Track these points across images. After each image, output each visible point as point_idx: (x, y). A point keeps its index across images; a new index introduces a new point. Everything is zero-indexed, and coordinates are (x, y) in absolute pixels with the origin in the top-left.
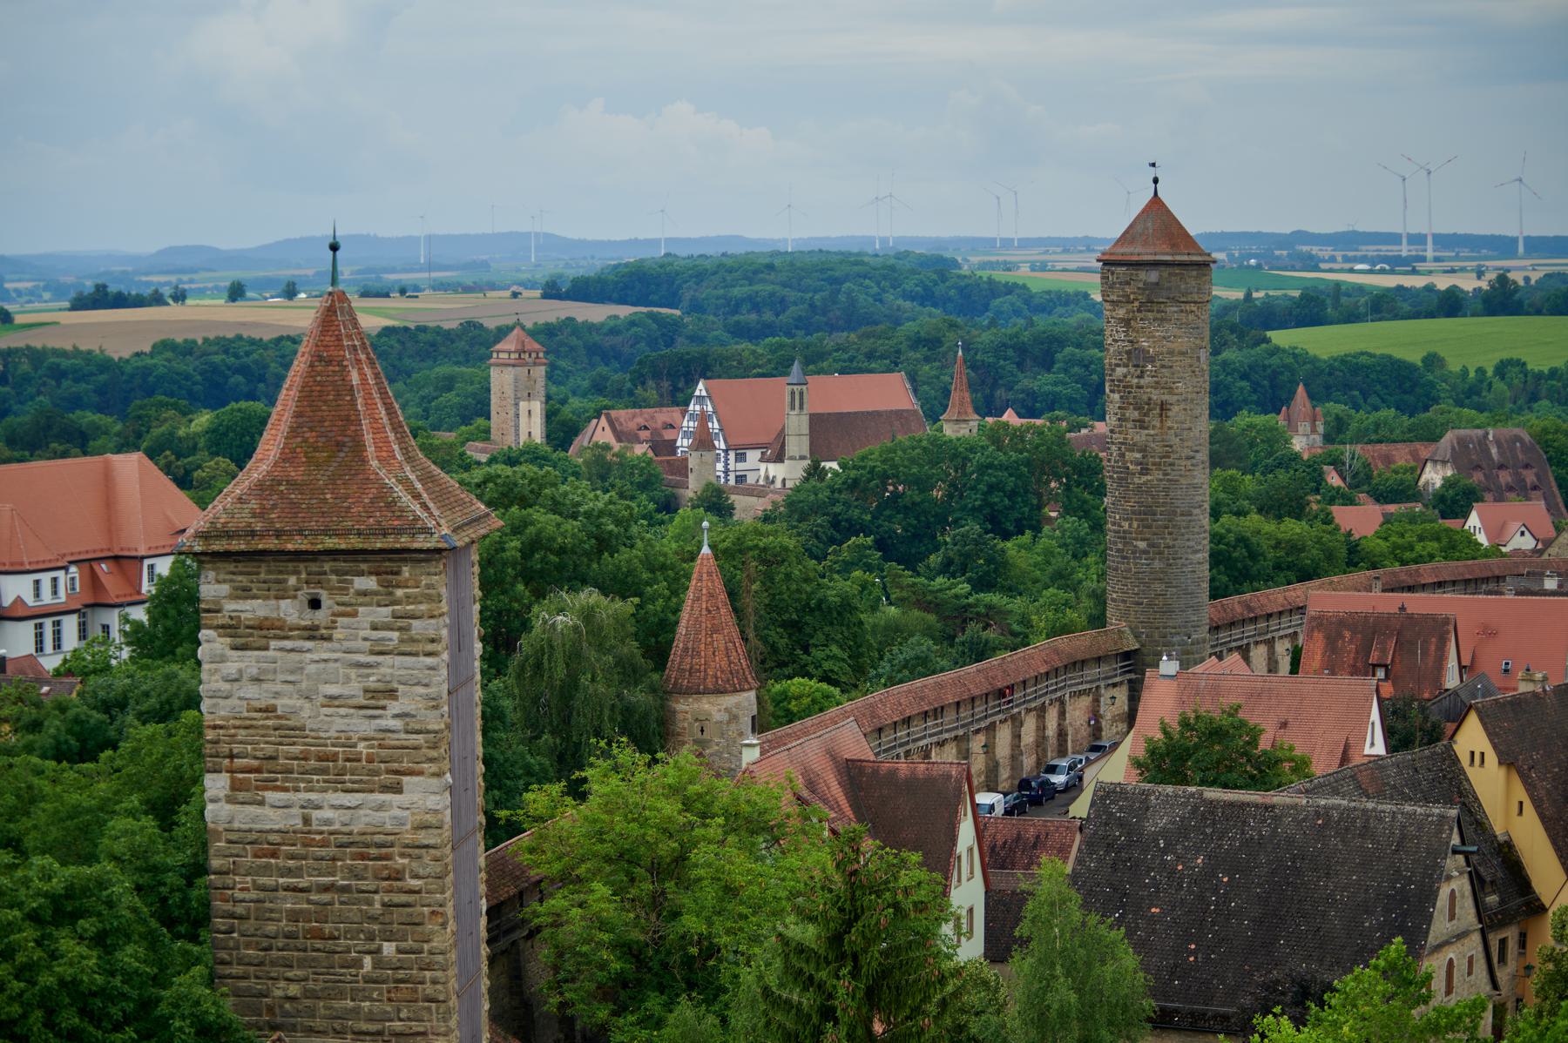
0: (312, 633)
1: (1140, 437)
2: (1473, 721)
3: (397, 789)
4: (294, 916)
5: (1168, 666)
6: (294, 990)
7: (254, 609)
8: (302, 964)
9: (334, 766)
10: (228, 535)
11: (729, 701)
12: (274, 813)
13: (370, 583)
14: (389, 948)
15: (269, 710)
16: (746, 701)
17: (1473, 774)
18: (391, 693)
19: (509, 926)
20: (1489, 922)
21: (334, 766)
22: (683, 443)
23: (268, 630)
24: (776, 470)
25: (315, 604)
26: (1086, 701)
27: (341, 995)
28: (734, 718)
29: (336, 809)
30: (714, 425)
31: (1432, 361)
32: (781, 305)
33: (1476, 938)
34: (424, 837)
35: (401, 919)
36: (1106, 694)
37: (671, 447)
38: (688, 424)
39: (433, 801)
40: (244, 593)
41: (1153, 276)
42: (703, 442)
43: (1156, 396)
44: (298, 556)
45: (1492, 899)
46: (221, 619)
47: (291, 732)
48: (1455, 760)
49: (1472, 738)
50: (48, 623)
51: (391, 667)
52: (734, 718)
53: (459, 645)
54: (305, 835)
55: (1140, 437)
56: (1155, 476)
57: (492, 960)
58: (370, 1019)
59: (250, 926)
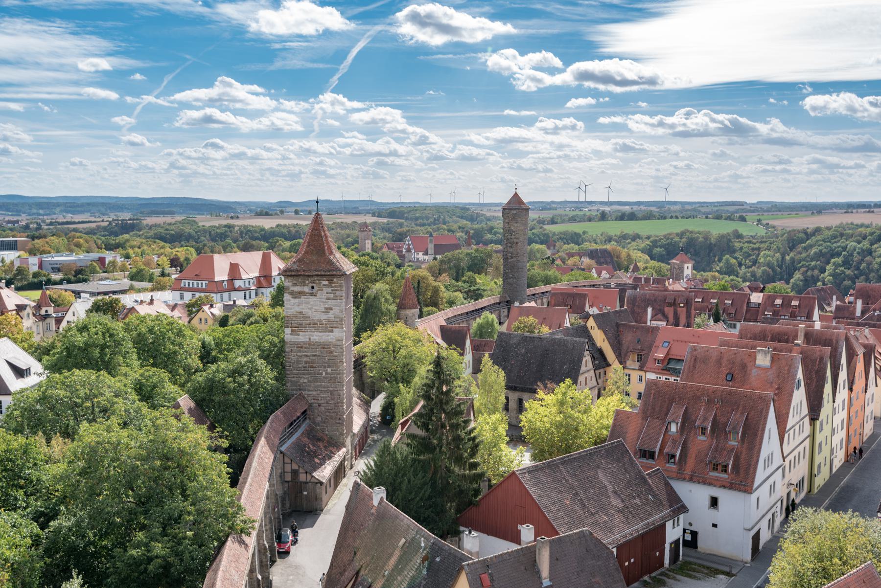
0: (312, 294)
1: (511, 250)
2: (591, 319)
3: (332, 331)
4: (306, 362)
5: (517, 304)
6: (305, 381)
7: (297, 289)
8: (308, 374)
9: (316, 326)
10: (291, 271)
11: (413, 311)
12: (302, 337)
13: (326, 283)
14: (329, 370)
15: (301, 313)
16: (417, 311)
17: (592, 331)
18: (331, 309)
19: (359, 364)
20: (596, 368)
21: (316, 326)
22: (404, 251)
23: (301, 293)
24: (426, 257)
25: (313, 288)
26: (497, 312)
27: (317, 381)
28: (414, 315)
29: (317, 337)
30: (411, 247)
31: (584, 233)
32: (427, 218)
33: (592, 372)
34: (338, 343)
35: (334, 363)
36: (502, 311)
37: (402, 252)
38: (406, 246)
39: (341, 334)
40: (295, 285)
41: (515, 212)
42: (409, 250)
43: (515, 240)
44: (309, 276)
45: (597, 362)
46: (289, 291)
47: (306, 318)
48: (587, 328)
49: (591, 323)
50: (247, 292)
51: (331, 303)
52: (414, 315)
53: (347, 298)
54: (310, 343)
55: (511, 250)
56: (514, 259)
57: (355, 373)
58: (324, 387)
59: (295, 365)
